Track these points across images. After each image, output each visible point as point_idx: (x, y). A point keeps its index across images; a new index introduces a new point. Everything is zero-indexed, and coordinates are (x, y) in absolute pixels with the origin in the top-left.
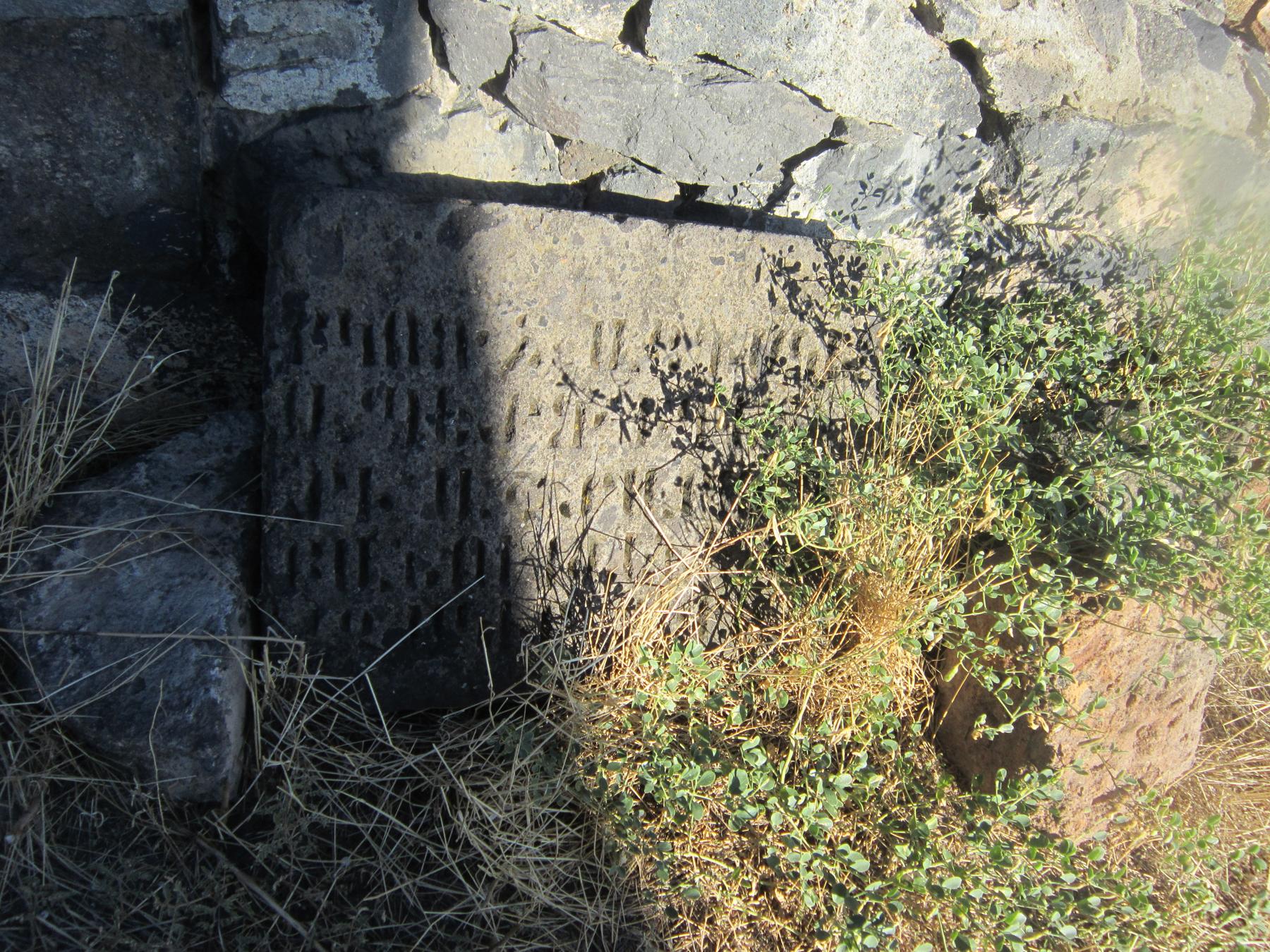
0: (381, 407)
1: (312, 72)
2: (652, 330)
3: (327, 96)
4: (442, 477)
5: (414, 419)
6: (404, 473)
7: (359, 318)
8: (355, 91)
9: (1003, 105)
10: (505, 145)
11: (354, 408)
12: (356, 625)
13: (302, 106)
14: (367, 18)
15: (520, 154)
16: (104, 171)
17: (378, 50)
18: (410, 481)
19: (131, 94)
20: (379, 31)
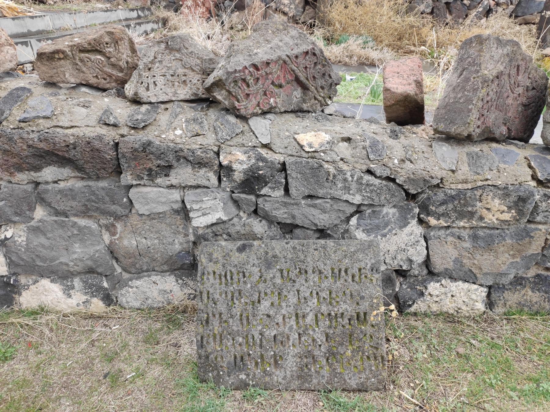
0: (224, 295)
1: (210, 216)
2: (298, 270)
3: (214, 221)
4: (241, 315)
5: (232, 300)
6: (230, 314)
7: (218, 272)
8: (220, 219)
9: (413, 192)
10: (262, 226)
11: (217, 296)
12: (219, 359)
13: (209, 224)
14: (219, 202)
15: (266, 228)
16: (169, 244)
17: (223, 208)
18: (232, 317)
19: (173, 227)
20: (222, 204)
